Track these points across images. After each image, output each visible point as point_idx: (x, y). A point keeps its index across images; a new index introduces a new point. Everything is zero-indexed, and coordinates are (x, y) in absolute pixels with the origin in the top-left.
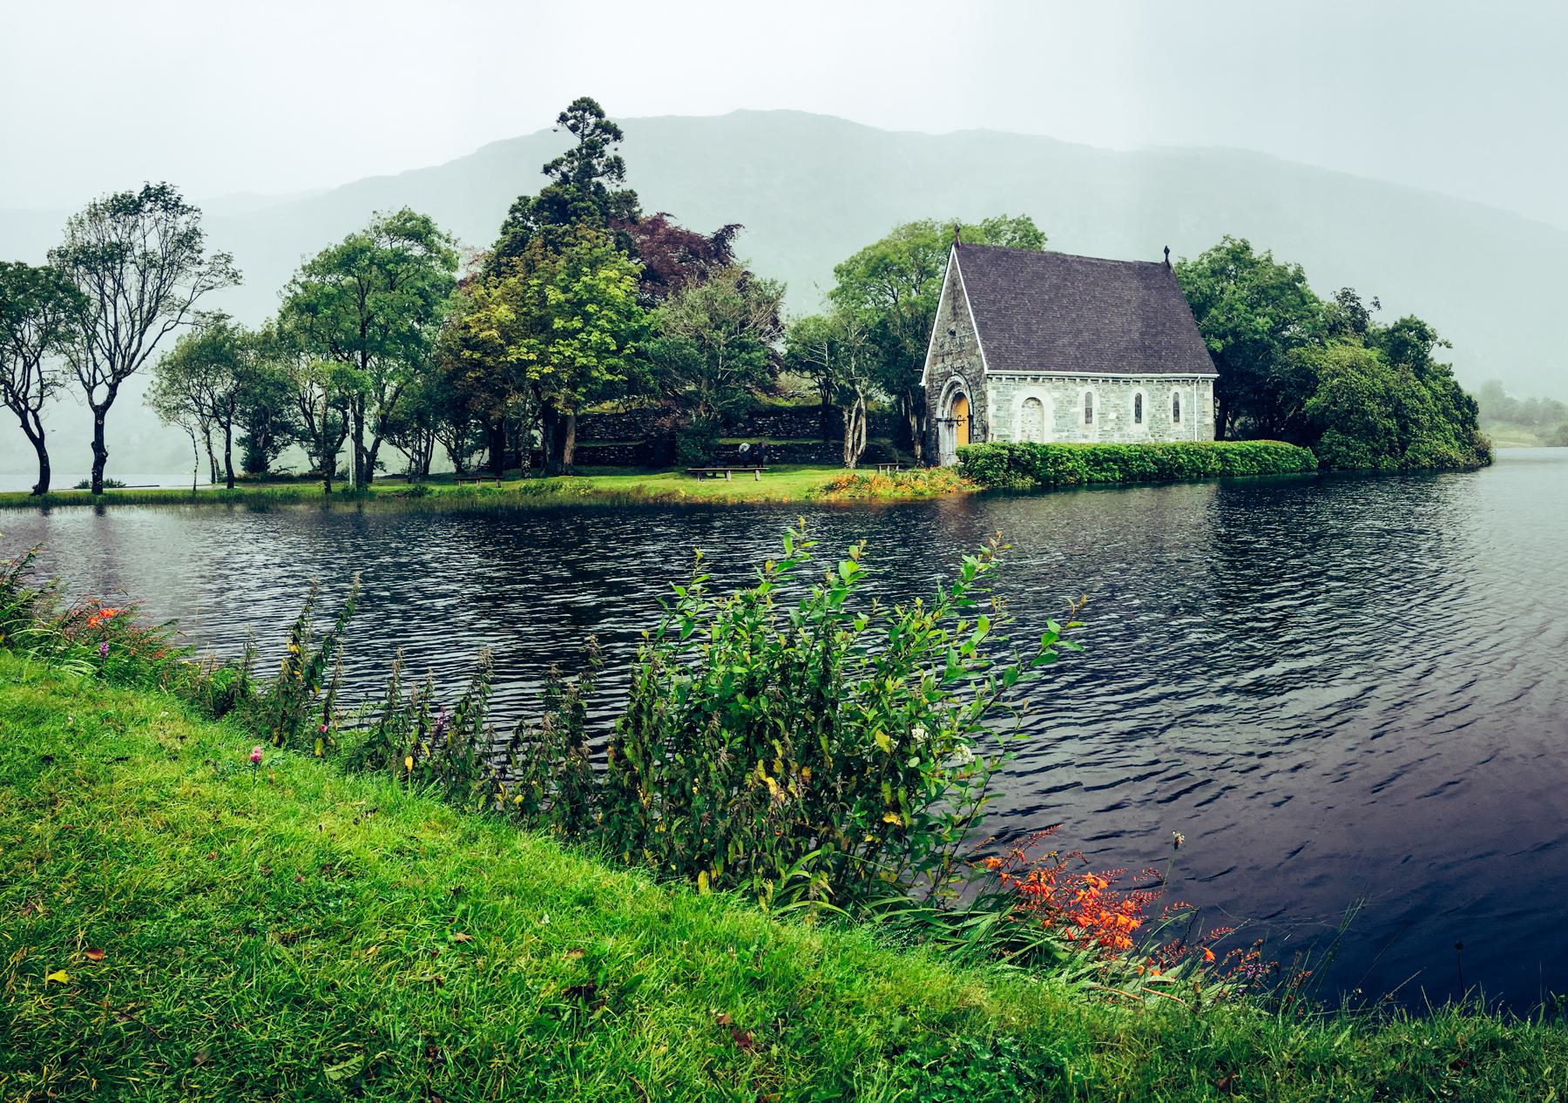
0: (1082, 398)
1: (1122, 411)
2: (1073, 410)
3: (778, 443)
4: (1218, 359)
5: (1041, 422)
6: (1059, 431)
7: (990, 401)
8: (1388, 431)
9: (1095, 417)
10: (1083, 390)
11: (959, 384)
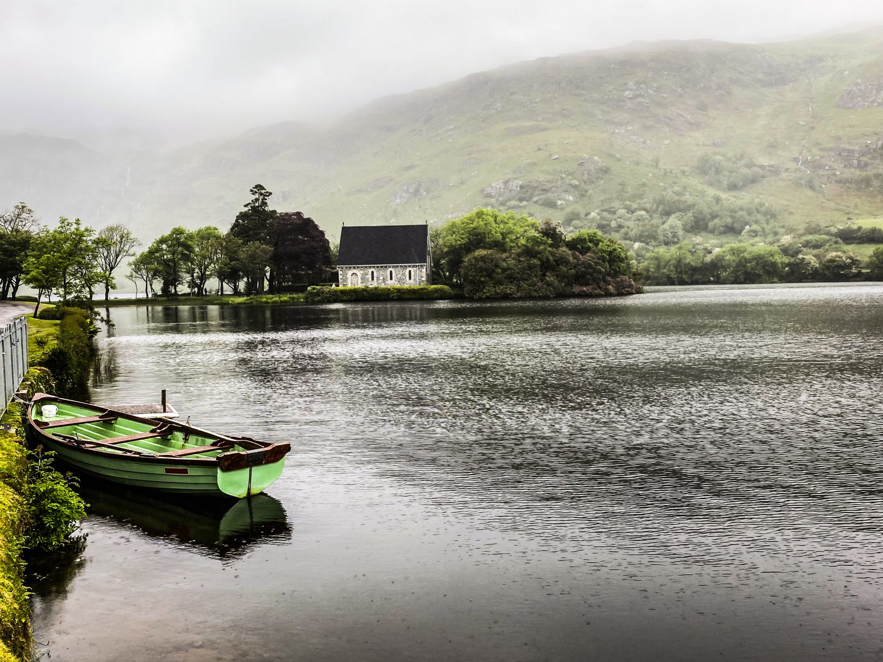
0: (370, 273)
2: (367, 277)
9: (375, 278)
10: (370, 271)
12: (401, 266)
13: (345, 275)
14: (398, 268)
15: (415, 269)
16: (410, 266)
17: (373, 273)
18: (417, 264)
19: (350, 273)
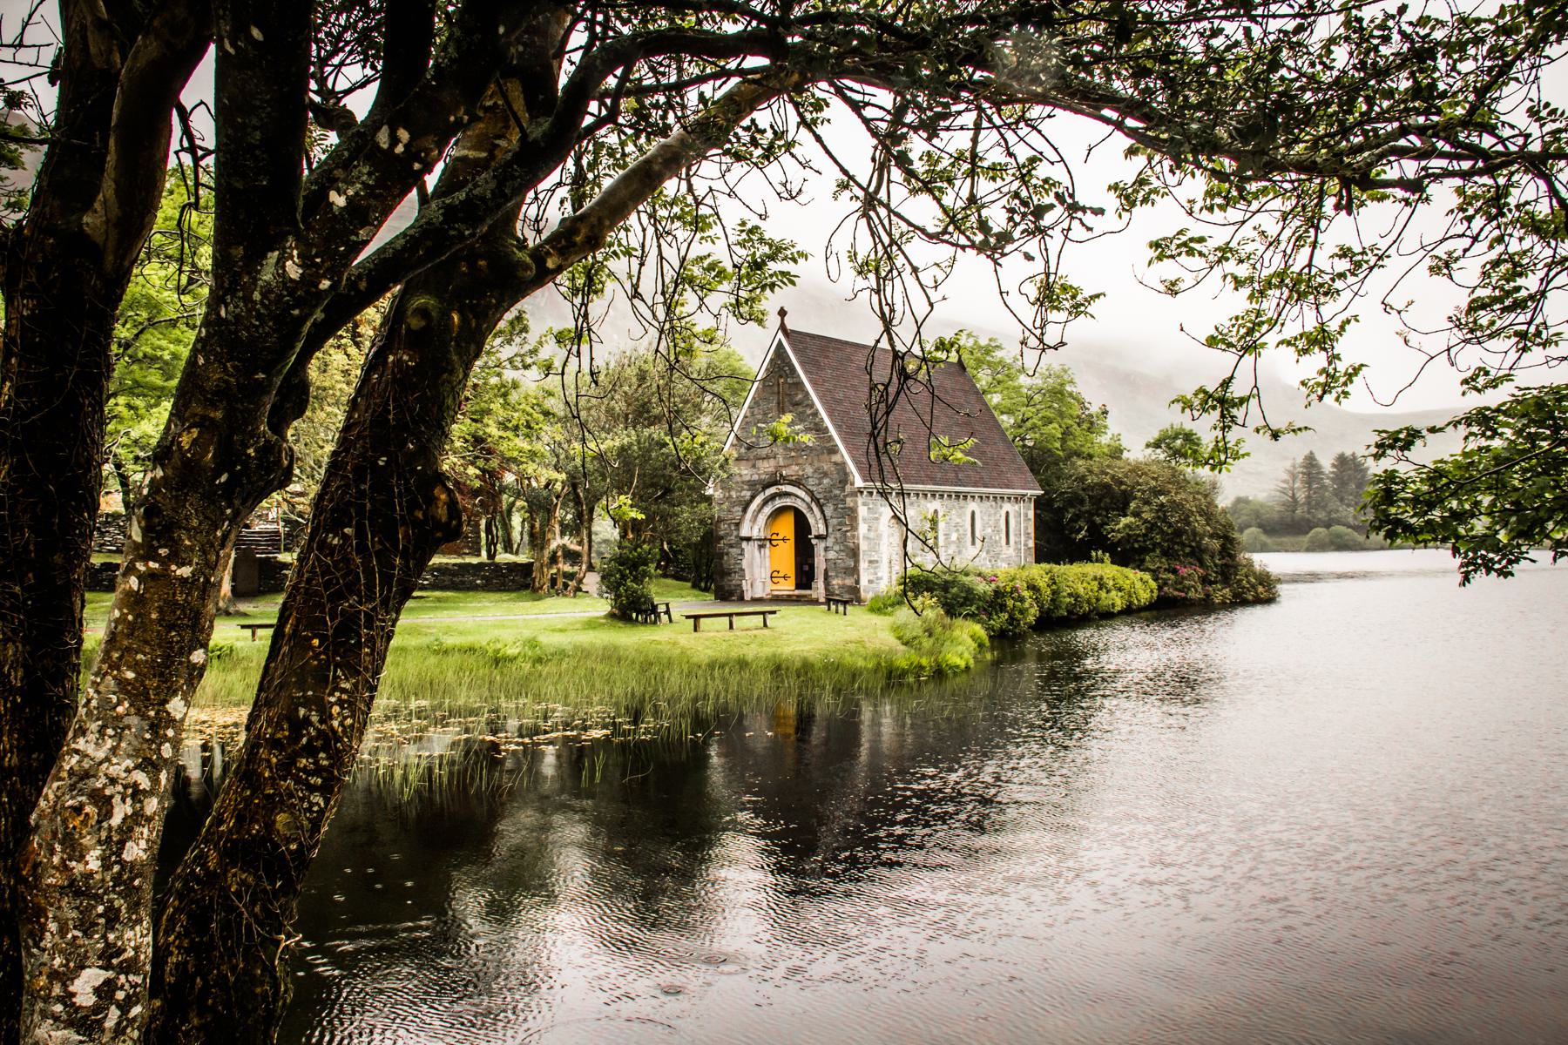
14: (986, 504)
15: (1017, 507)
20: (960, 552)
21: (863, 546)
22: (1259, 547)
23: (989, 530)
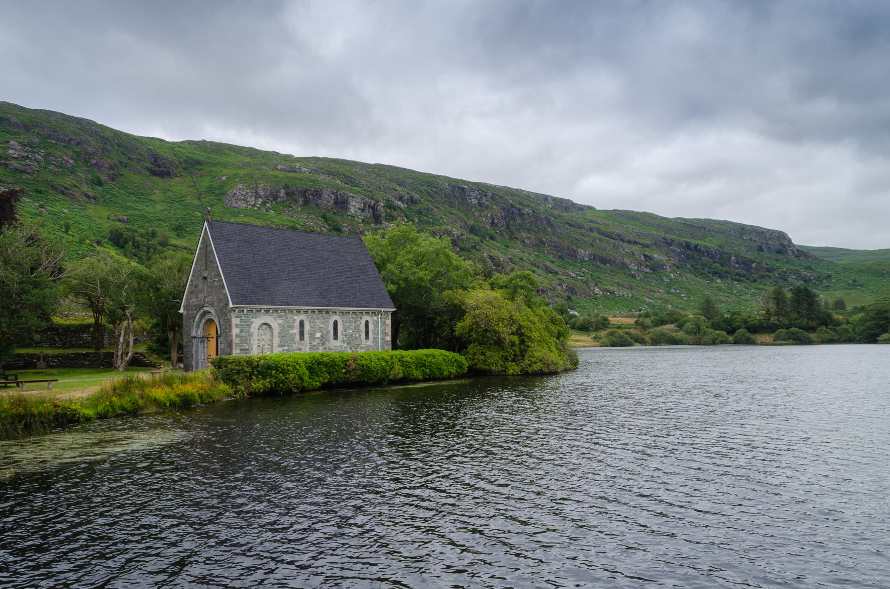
0: (297, 324)
1: (324, 332)
2: (291, 332)
3: (56, 352)
4: (393, 297)
5: (271, 340)
6: (282, 346)
7: (234, 325)
8: (513, 344)
9: (306, 336)
10: (298, 318)
11: (209, 312)
12: (354, 313)
13: (245, 327)
15: (375, 318)
16: (367, 313)
17: (302, 324)
18: (383, 310)
19: (257, 322)
20: (323, 344)
21: (235, 340)
22: (710, 342)
23: (351, 331)
